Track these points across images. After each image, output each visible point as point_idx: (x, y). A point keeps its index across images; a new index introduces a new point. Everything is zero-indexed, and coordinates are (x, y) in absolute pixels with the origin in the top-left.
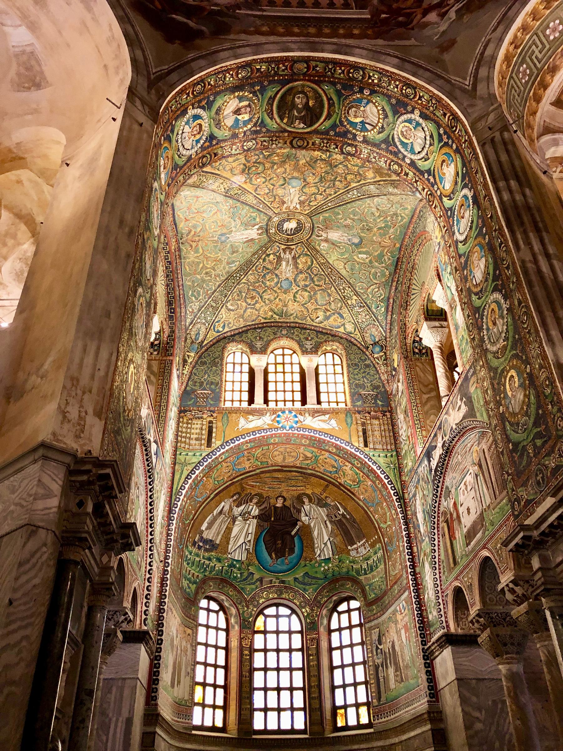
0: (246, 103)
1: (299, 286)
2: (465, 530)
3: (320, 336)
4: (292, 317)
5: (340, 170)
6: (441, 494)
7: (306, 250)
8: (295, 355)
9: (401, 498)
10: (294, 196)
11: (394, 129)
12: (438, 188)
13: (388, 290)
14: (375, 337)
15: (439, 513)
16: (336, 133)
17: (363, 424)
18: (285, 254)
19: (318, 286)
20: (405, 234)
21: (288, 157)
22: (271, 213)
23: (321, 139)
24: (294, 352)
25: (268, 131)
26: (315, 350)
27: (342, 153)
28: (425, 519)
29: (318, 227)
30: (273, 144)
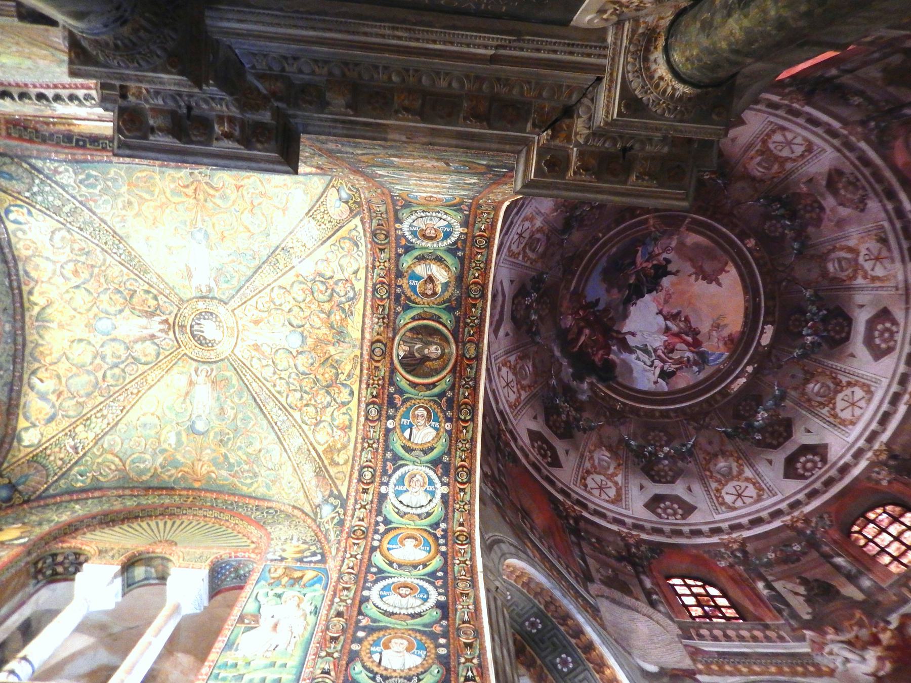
0: (439, 289)
1: (102, 346)
4: (36, 337)
7: (167, 353)
11: (414, 463)
13: (113, 485)
14: (24, 483)
18: (160, 323)
19: (104, 376)
20: (220, 492)
21: (340, 333)
22: (234, 303)
23: (383, 378)
25: (397, 314)
27: (367, 405)
29: (212, 370)
30: (379, 319)
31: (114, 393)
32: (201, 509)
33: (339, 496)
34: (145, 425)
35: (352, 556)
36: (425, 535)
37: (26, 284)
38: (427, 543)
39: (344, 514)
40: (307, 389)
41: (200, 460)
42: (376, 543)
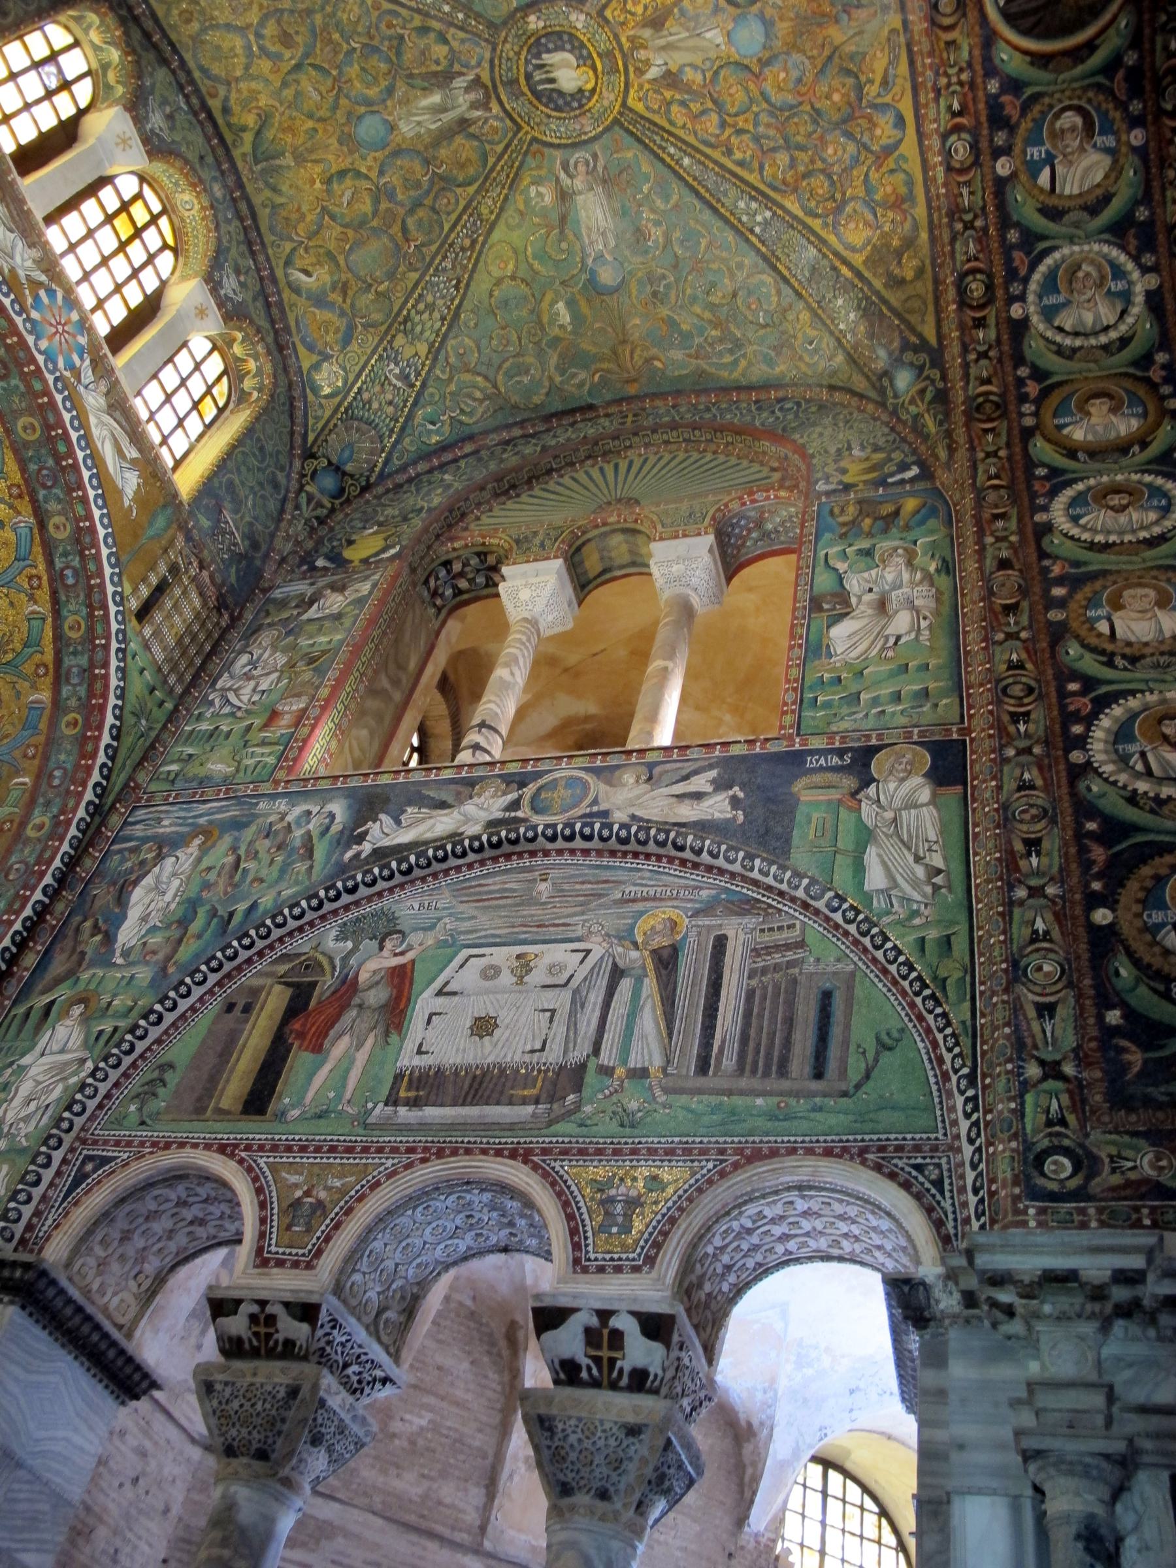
1: (381, 173)
2: (408, 1060)
3: (259, 304)
4: (268, 193)
5: (838, 150)
6: (335, 912)
7: (499, 148)
8: (168, 256)
9: (98, 811)
10: (695, 49)
11: (1072, 240)
12: (1036, 414)
14: (350, 459)
15: (271, 947)
16: (996, 97)
17: (174, 569)
18: (467, 90)
19: (405, 230)
20: (678, 393)
23: (970, 65)
24: (175, 251)
26: (232, 313)
27: (944, 137)
28: (183, 923)
29: (595, 156)
31: (433, 258)
32: (654, 431)
33: (923, 346)
34: (506, 303)
35: (988, 455)
36: (1128, 384)
37: (214, 96)
38: (1135, 400)
39: (944, 378)
40: (799, 138)
41: (624, 342)
42: (1029, 422)
